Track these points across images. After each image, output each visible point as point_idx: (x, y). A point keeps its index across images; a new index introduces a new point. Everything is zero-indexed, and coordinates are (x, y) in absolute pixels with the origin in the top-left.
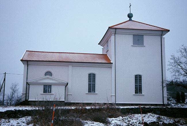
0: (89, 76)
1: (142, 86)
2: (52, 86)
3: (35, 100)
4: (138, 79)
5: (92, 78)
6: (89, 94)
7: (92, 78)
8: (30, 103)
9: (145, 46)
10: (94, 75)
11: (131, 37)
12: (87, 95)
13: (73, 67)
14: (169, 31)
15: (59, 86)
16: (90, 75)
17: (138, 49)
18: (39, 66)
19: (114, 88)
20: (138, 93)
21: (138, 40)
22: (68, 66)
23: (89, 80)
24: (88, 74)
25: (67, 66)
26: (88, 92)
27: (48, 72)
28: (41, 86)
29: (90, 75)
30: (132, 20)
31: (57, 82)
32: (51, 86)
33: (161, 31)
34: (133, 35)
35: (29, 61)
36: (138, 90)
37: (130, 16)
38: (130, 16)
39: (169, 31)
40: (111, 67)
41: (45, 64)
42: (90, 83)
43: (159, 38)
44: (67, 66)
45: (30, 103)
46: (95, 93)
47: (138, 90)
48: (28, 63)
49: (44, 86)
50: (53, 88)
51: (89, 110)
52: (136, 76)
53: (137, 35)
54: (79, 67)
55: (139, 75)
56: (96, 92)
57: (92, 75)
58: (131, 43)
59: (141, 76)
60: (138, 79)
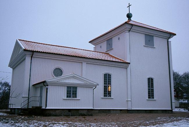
0: (105, 77)
1: (154, 90)
2: (78, 88)
3: (93, 108)
4: (150, 81)
5: (107, 79)
6: (69, 100)
7: (107, 79)
8: (47, 112)
9: (155, 48)
10: (109, 76)
11: (143, 36)
12: (65, 101)
13: (87, 64)
14: (175, 35)
15: (87, 88)
16: (105, 75)
17: (149, 50)
18: (39, 59)
19: (128, 92)
20: (151, 98)
21: (149, 41)
22: (82, 63)
23: (104, 81)
24: (103, 75)
25: (81, 62)
26: (103, 96)
27: (57, 69)
28: (64, 87)
29: (105, 75)
30: (132, 20)
31: (84, 83)
32: (76, 88)
33: (169, 34)
34: (146, 35)
35: (36, 51)
36: (151, 95)
37: (129, 16)
38: (129, 16)
39: (175, 35)
40: (127, 68)
41: (74, 60)
42: (152, 88)
43: (166, 41)
44: (81, 62)
45: (47, 112)
46: (77, 99)
47: (151, 95)
48: (33, 55)
49: (68, 87)
50: (79, 91)
51: (56, 122)
52: (149, 79)
53: (148, 35)
54: (120, 68)
55: (151, 79)
56: (112, 97)
57: (150, 80)
58: (144, 44)
59: (110, 75)
60: (150, 81)
